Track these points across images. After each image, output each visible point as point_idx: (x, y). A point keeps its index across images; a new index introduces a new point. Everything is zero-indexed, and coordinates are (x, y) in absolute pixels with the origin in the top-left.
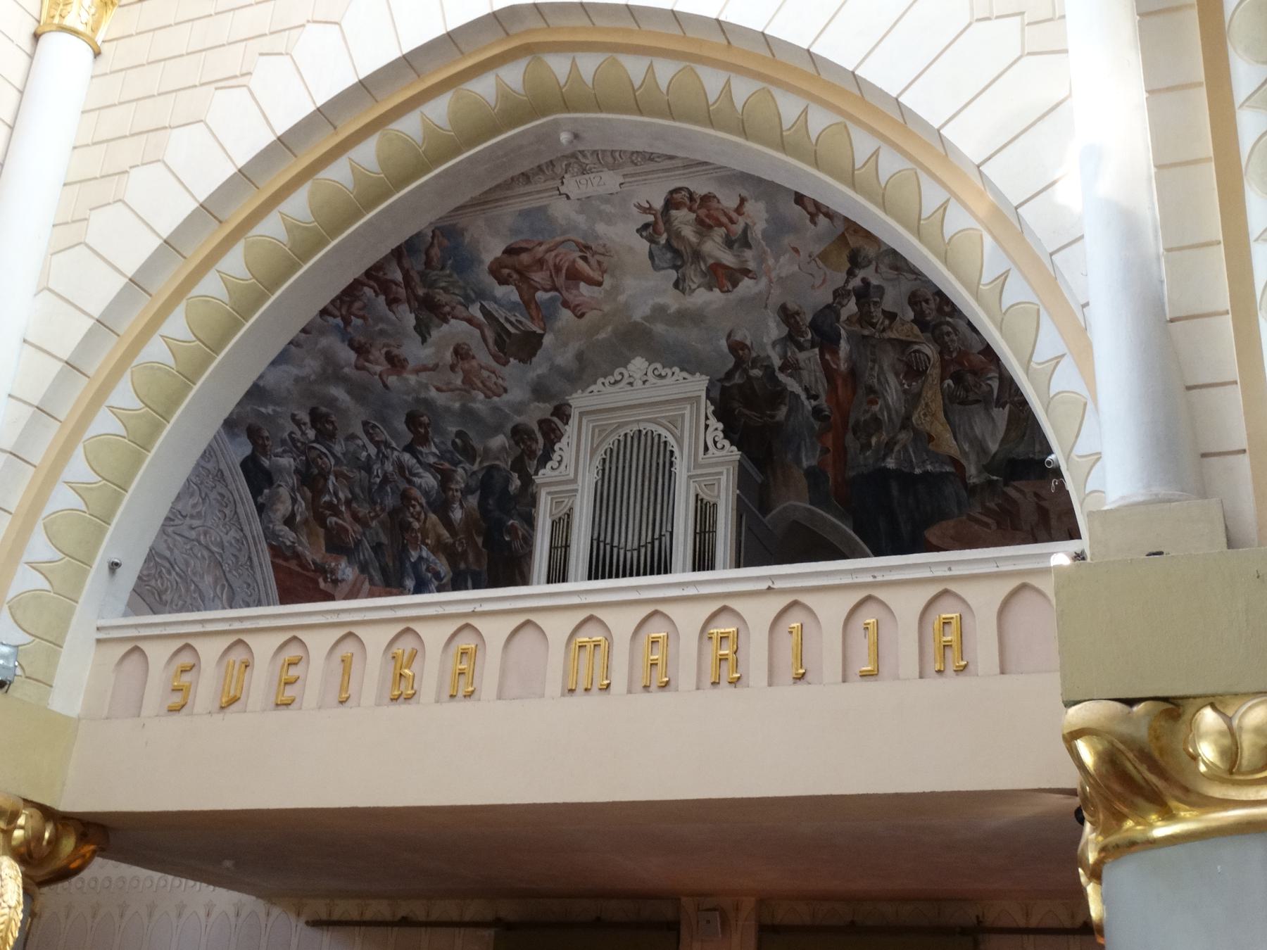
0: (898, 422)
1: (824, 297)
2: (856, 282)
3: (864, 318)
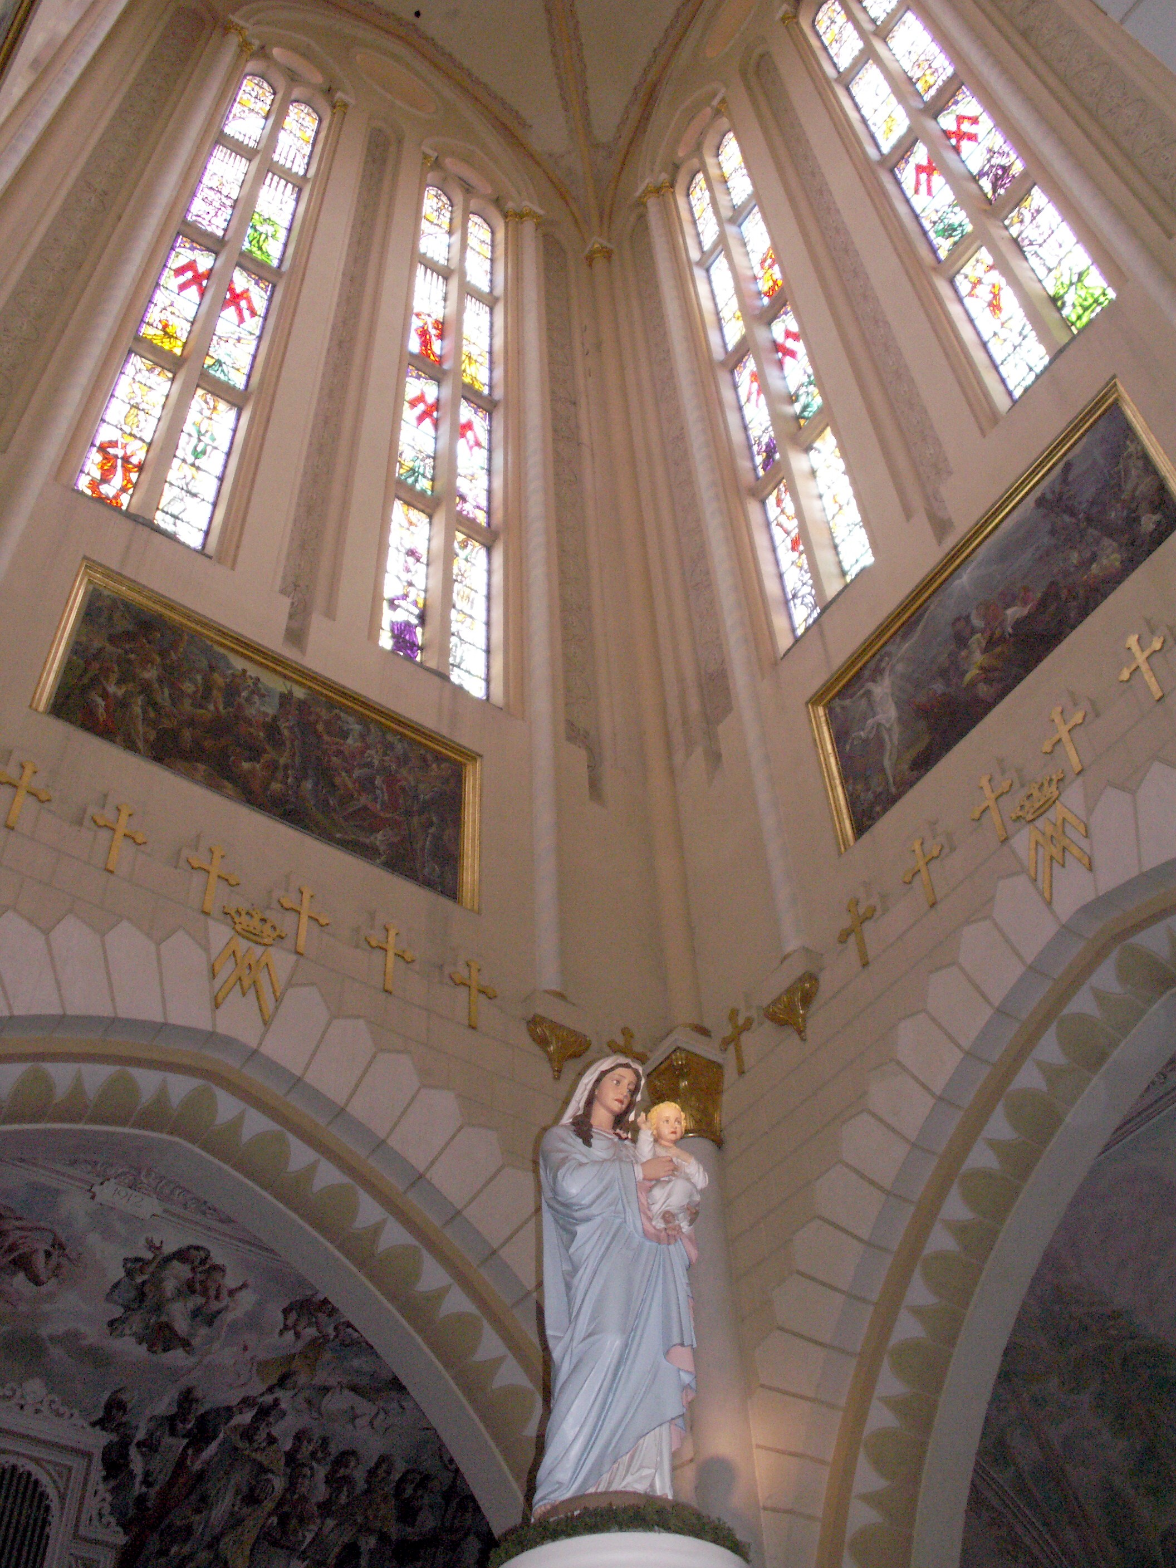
0: (207, 1538)
1: (233, 1398)
2: (269, 1399)
3: (248, 1433)
